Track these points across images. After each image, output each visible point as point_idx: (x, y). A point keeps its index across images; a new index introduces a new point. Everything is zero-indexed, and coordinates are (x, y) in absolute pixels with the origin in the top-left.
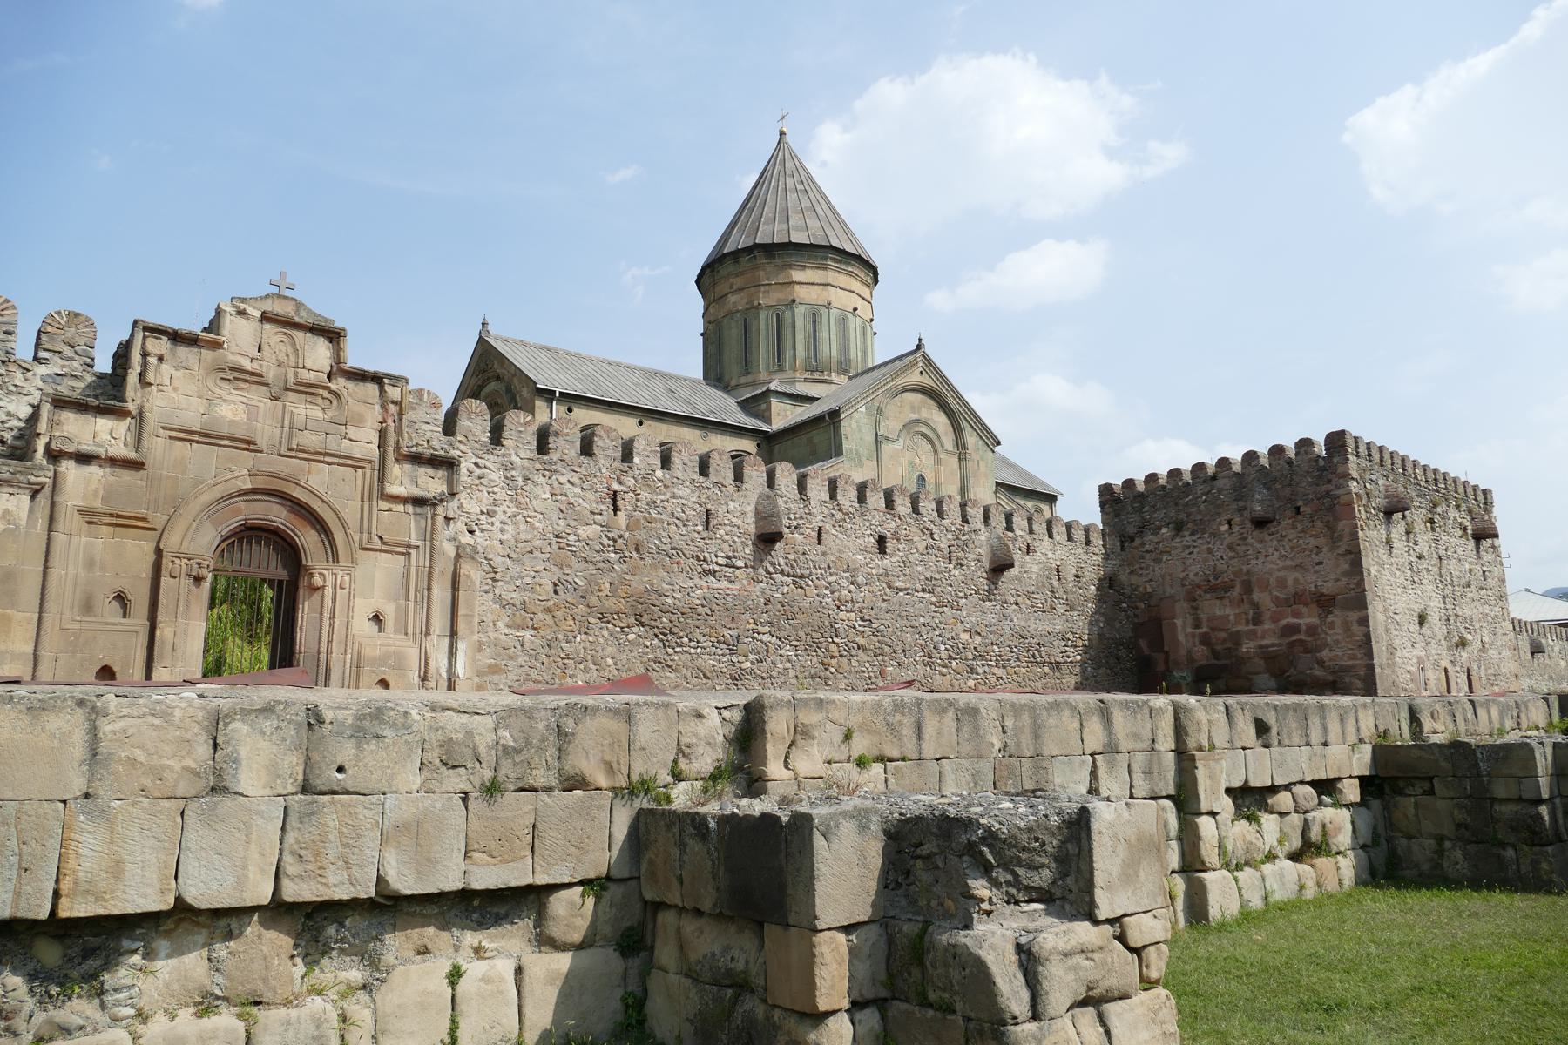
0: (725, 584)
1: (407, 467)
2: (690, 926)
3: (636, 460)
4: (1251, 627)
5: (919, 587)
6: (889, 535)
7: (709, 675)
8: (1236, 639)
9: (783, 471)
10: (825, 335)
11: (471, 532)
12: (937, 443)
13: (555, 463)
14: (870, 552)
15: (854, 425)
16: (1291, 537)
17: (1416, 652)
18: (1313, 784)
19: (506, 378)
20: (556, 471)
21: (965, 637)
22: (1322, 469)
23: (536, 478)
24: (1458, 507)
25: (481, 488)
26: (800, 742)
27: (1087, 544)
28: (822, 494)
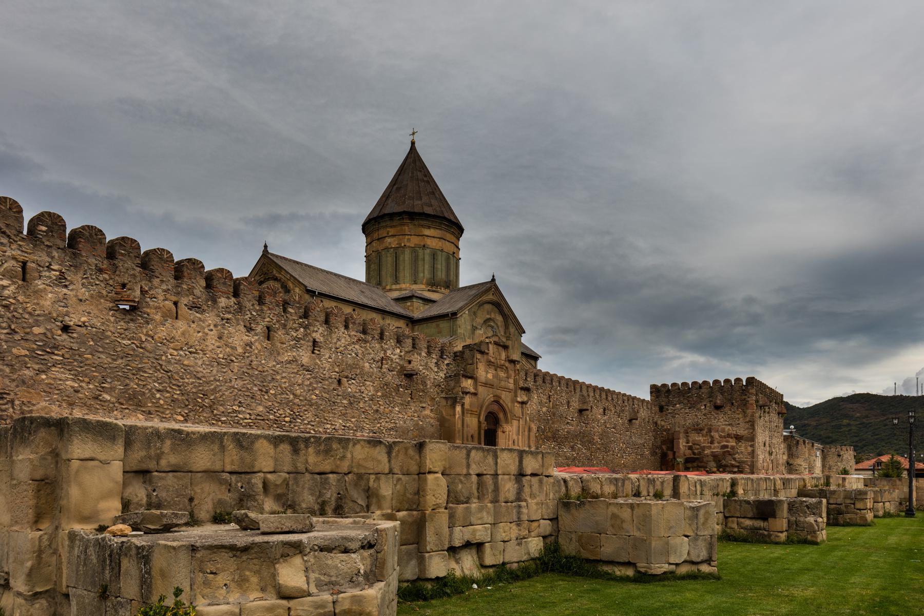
8: (703, 448)
15: (463, 321)
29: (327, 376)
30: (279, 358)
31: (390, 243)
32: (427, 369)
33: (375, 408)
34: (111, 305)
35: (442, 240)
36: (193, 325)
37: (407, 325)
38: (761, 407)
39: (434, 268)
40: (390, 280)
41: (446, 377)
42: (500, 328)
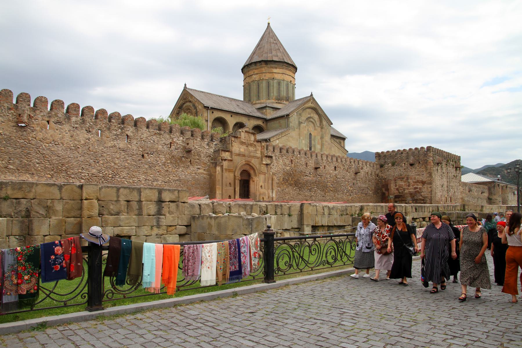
1: (265, 158)
3: (295, 153)
8: (404, 190)
10: (282, 89)
12: (315, 124)
17: (441, 194)
18: (422, 218)
19: (193, 102)
20: (283, 156)
22: (425, 154)
24: (453, 161)
29: (135, 153)
30: (105, 145)
31: (255, 78)
32: (202, 147)
33: (166, 169)
34: (15, 124)
35: (284, 74)
36: (57, 131)
37: (263, 123)
38: (438, 164)
39: (279, 90)
40: (255, 98)
41: (214, 152)
42: (317, 122)
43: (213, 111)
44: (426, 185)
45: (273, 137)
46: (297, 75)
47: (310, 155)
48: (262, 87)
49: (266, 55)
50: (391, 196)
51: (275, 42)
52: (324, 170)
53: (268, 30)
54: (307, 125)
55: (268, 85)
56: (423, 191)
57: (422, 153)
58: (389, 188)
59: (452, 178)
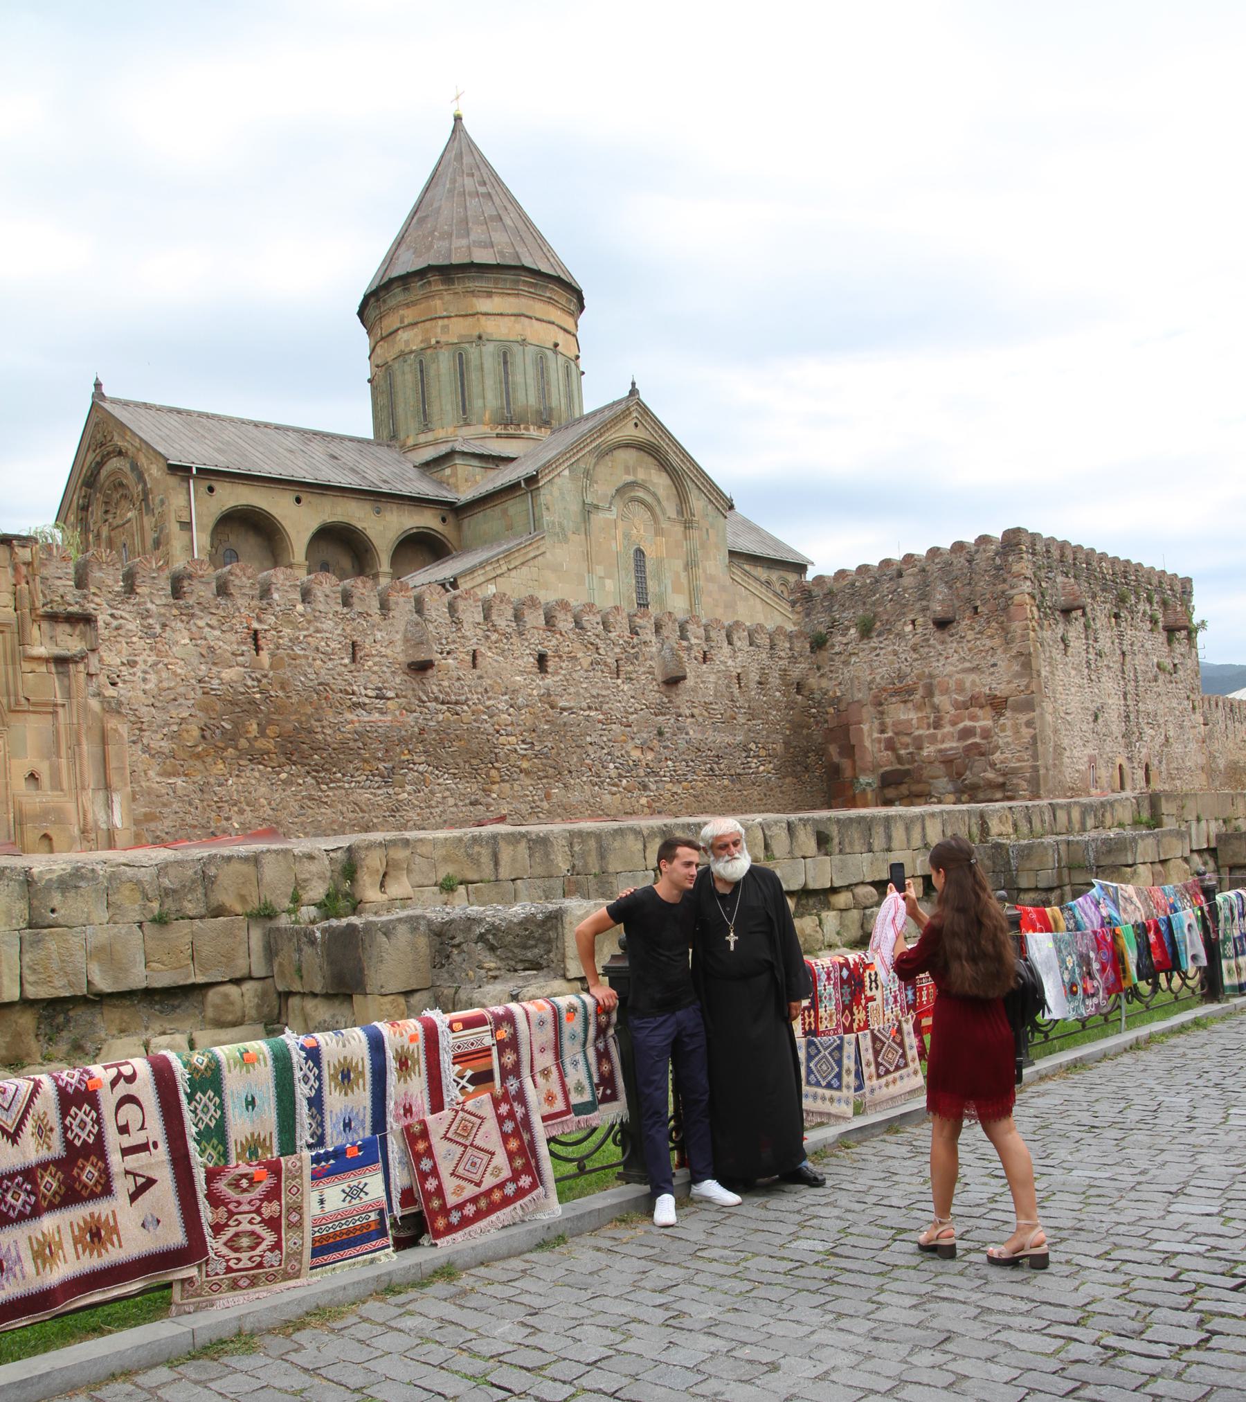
0: (376, 716)
1: (45, 625)
2: (310, 1004)
3: (276, 596)
4: (932, 731)
5: (584, 705)
6: (550, 653)
7: (365, 808)
9: (432, 594)
10: (519, 379)
11: (114, 684)
12: (657, 509)
13: (192, 607)
14: (530, 673)
15: (556, 493)
16: (969, 638)
17: (1089, 751)
20: (193, 615)
21: (636, 754)
22: (998, 568)
23: (173, 624)
24: (1149, 600)
25: (119, 639)
26: (392, 873)
27: (772, 648)
28: (476, 615)
31: (407, 343)
37: (444, 520)
38: (1066, 612)
39: (507, 383)
40: (413, 425)
42: (665, 503)
43: (214, 484)
44: (1008, 713)
45: (471, 571)
46: (583, 319)
47: (376, 604)
48: (439, 375)
49: (445, 244)
50: (863, 779)
51: (482, 190)
52: (470, 676)
53: (456, 144)
54: (623, 517)
55: (461, 364)
56: (1001, 742)
57: (983, 565)
58: (853, 742)
59: (1150, 675)
